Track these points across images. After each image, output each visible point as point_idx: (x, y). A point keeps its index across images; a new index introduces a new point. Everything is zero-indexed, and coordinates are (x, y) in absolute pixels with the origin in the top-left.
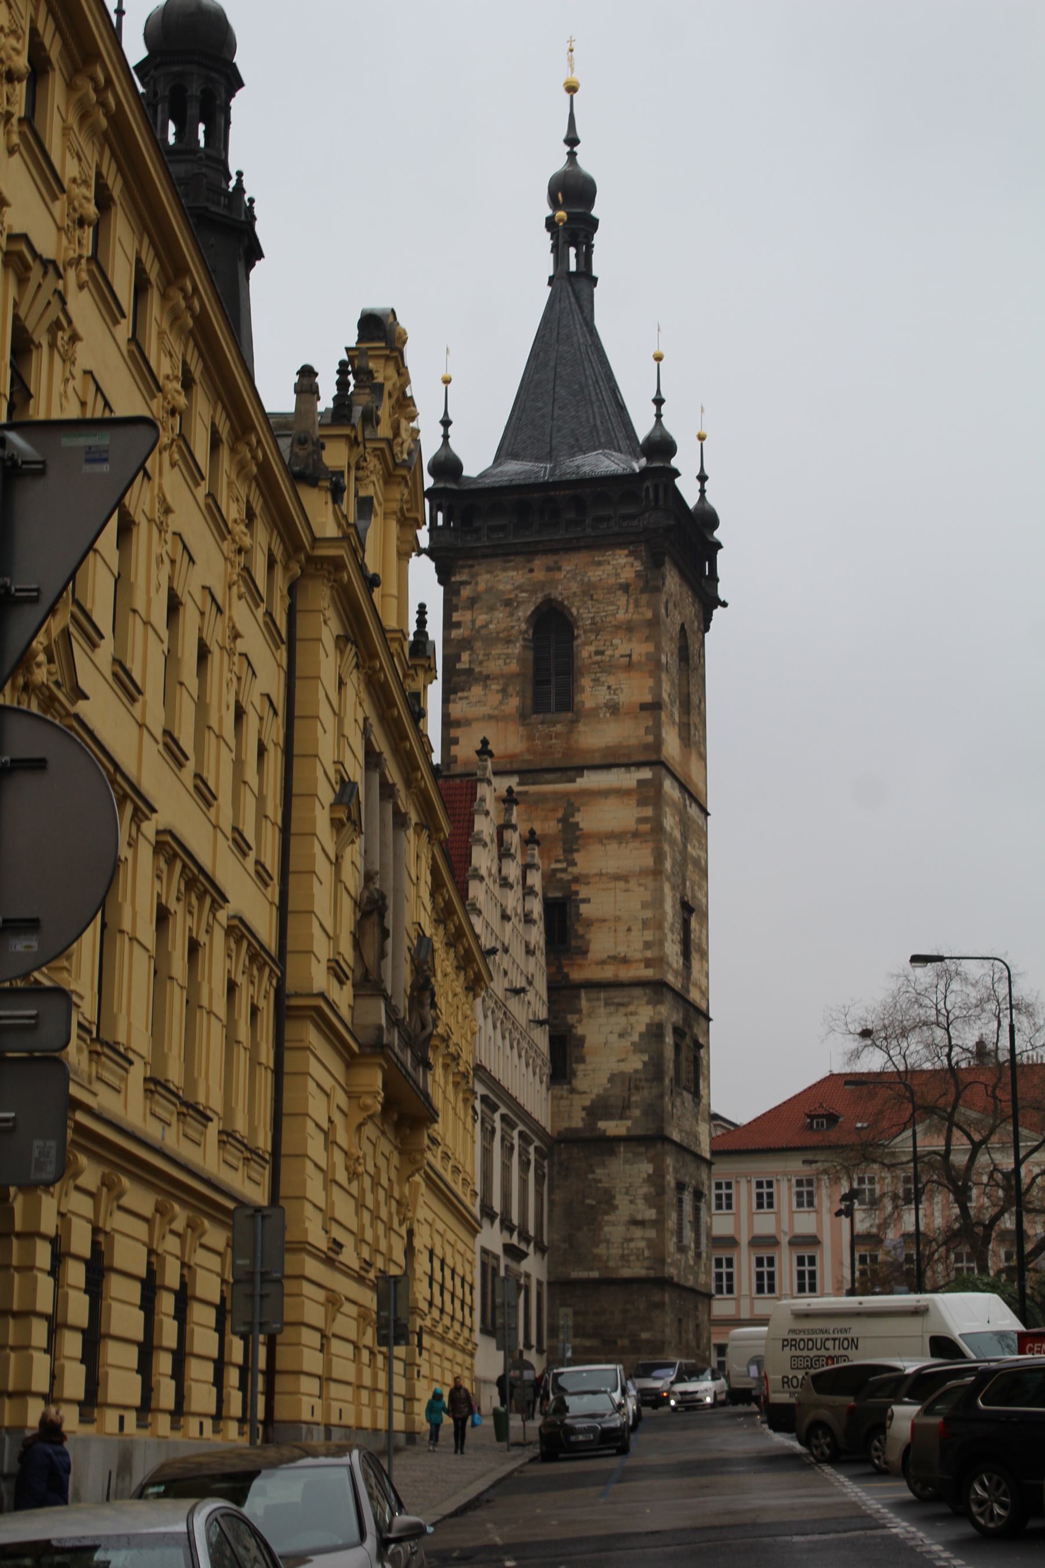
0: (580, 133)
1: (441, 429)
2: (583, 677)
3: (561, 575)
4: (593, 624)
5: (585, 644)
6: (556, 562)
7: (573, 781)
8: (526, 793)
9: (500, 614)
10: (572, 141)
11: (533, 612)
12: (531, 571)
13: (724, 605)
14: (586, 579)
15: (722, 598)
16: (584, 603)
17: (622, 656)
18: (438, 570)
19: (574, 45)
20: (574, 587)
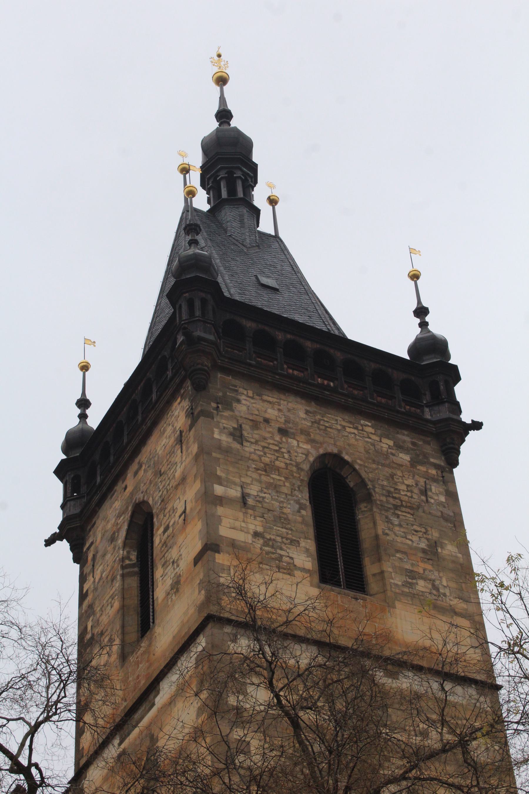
1: (78, 411)
2: (157, 569)
3: (141, 473)
4: (163, 501)
5: (158, 529)
6: (139, 463)
7: (153, 704)
9: (108, 556)
11: (128, 531)
12: (125, 488)
13: (477, 426)
14: (156, 459)
15: (466, 417)
16: (156, 484)
17: (180, 516)
18: (72, 549)
19: (221, 52)
20: (150, 474)
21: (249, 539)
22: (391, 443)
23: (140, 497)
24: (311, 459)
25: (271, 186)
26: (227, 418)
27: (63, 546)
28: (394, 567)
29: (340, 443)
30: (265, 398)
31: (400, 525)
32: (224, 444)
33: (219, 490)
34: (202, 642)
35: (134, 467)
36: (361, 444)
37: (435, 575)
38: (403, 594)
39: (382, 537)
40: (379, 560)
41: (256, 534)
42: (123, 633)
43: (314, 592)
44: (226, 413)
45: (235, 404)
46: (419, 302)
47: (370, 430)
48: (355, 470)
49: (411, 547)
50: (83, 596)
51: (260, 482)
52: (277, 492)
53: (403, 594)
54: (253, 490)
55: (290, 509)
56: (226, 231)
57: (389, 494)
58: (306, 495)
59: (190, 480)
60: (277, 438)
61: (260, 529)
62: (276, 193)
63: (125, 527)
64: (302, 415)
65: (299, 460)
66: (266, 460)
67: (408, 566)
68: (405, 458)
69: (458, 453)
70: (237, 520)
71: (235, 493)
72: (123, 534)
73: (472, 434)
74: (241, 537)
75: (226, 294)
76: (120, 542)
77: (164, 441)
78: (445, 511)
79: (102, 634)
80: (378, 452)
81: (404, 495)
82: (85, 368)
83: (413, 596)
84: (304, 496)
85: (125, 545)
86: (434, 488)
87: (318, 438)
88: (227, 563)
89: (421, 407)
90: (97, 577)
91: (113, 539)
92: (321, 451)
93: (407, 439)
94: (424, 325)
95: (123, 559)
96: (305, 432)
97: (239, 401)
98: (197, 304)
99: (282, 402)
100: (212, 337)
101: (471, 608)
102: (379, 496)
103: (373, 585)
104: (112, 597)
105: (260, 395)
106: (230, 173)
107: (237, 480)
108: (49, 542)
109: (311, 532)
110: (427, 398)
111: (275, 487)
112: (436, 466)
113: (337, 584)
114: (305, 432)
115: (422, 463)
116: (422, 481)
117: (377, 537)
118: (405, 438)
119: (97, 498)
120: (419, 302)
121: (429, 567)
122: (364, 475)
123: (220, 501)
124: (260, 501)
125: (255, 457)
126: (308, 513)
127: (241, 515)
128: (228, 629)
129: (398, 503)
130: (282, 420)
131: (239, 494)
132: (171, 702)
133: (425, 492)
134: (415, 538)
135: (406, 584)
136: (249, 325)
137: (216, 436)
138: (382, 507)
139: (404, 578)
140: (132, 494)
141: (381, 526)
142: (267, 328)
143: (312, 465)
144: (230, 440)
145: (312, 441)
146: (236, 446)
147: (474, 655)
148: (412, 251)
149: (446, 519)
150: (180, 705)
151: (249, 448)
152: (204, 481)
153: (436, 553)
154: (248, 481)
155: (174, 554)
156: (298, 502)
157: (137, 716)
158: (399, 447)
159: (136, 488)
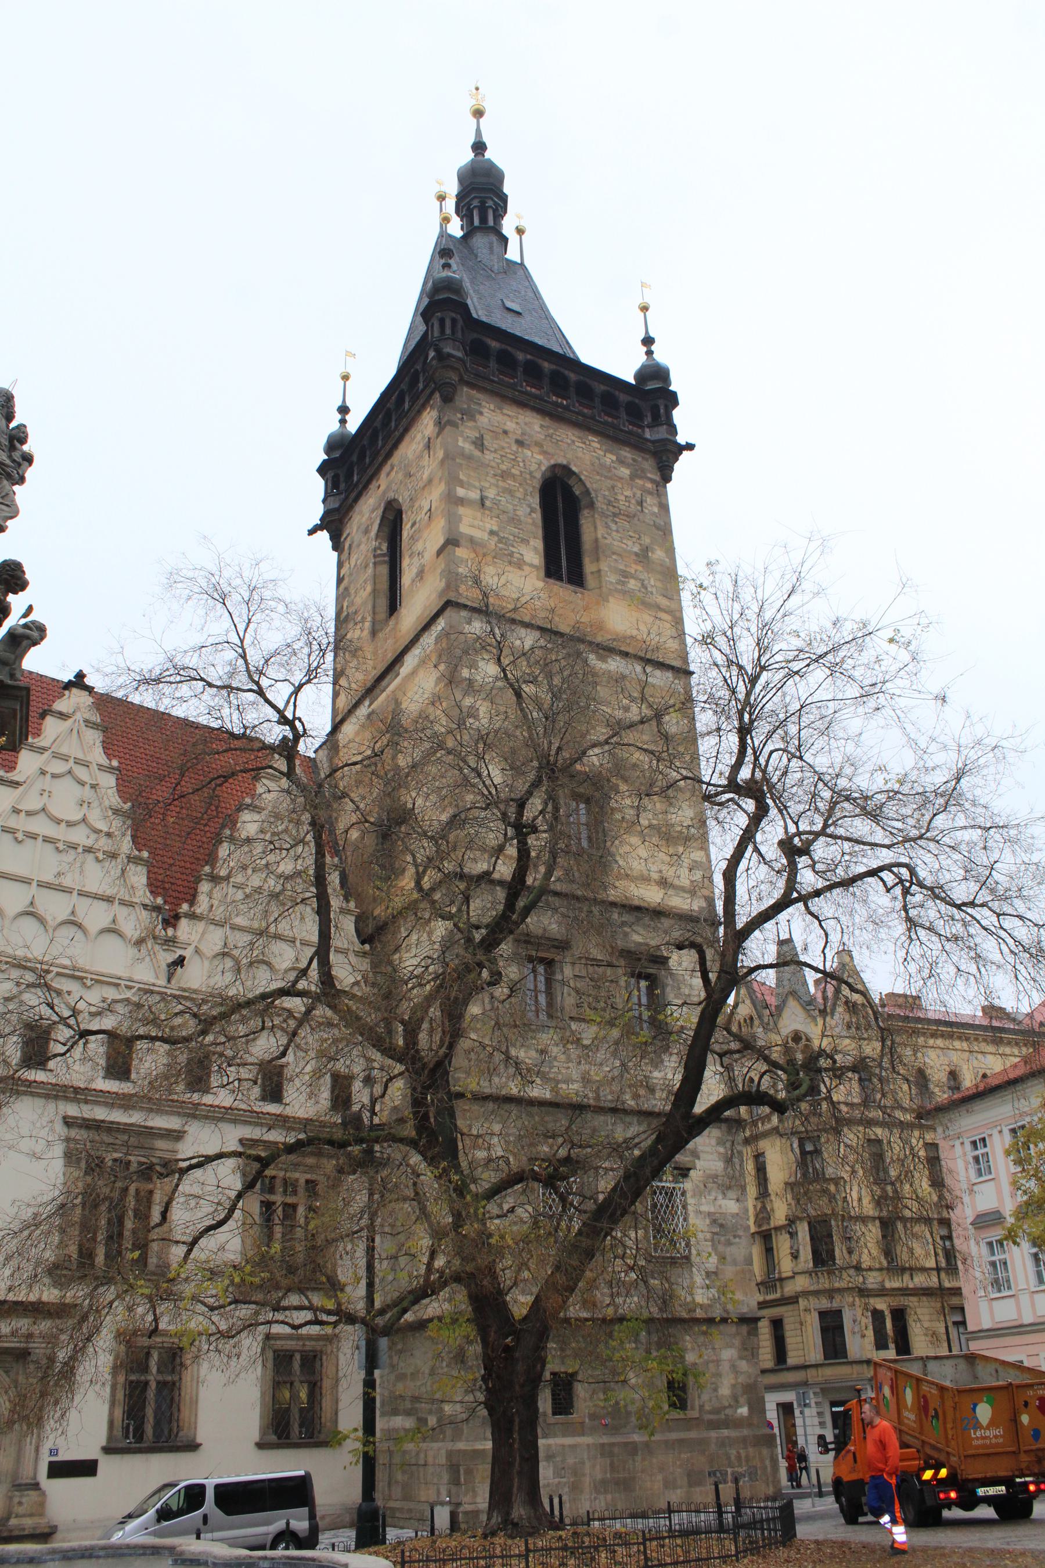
3: (393, 474)
8: (373, 712)
9: (363, 547)
10: (479, 147)
11: (380, 525)
13: (690, 447)
15: (681, 439)
18: (331, 539)
20: (400, 476)
21: (486, 537)
22: (614, 458)
23: (391, 495)
24: (543, 468)
25: (519, 217)
26: (470, 428)
27: (324, 536)
28: (610, 567)
29: (569, 456)
31: (617, 531)
32: (467, 451)
33: (461, 492)
34: (441, 624)
35: (386, 468)
36: (587, 457)
37: (644, 576)
38: (616, 590)
39: (602, 541)
40: (598, 560)
41: (492, 533)
42: (374, 613)
43: (540, 584)
44: (470, 424)
45: (478, 416)
46: (647, 332)
48: (580, 480)
49: (625, 550)
50: (340, 580)
51: (497, 486)
53: (616, 590)
54: (491, 493)
55: (522, 511)
56: (476, 256)
57: (609, 503)
58: (537, 500)
59: (436, 481)
60: (514, 447)
61: (495, 528)
62: (523, 223)
63: (378, 522)
64: (537, 428)
65: (534, 467)
66: (504, 467)
67: (622, 567)
68: (625, 472)
69: (672, 470)
70: (475, 519)
71: (474, 495)
73: (685, 453)
74: (478, 534)
75: (475, 315)
76: (373, 533)
77: (414, 446)
78: (658, 521)
79: (356, 613)
80: (602, 466)
81: (622, 504)
82: (346, 378)
83: (624, 593)
84: (535, 501)
85: (377, 536)
86: (649, 500)
87: (551, 450)
88: (465, 556)
89: (642, 427)
90: (353, 564)
91: (367, 531)
92: (552, 462)
93: (629, 455)
94: (649, 353)
95: (375, 550)
96: (538, 444)
97: (481, 413)
98: (448, 323)
100: (459, 354)
101: (673, 606)
102: (600, 504)
103: (590, 581)
104: (365, 582)
105: (500, 409)
106: (483, 203)
107: (477, 484)
109: (540, 533)
110: (648, 420)
111: (510, 492)
112: (652, 481)
113: (560, 579)
114: (538, 444)
115: (641, 478)
116: (639, 493)
117: (596, 540)
118: (627, 454)
119: (353, 495)
120: (647, 332)
121: (640, 568)
122: (588, 485)
123: (461, 501)
124: (497, 503)
125: (493, 464)
126: (538, 516)
127: (479, 514)
128: (464, 613)
129: (617, 511)
130: (519, 432)
131: (478, 497)
132: (414, 672)
133: (641, 503)
134: (630, 543)
135: (619, 582)
136: (494, 344)
137: (460, 444)
138: (603, 514)
139: (618, 577)
140: (384, 493)
141: (601, 532)
142: (509, 349)
143: (543, 474)
144: (472, 448)
145: (544, 453)
146: (477, 453)
147: (673, 645)
148: (643, 285)
149: (658, 528)
150: (421, 673)
151: (489, 456)
152: (448, 484)
153: (646, 557)
154: (487, 485)
155: (419, 546)
156: (529, 506)
157: (384, 683)
158: (621, 462)
159: (388, 488)
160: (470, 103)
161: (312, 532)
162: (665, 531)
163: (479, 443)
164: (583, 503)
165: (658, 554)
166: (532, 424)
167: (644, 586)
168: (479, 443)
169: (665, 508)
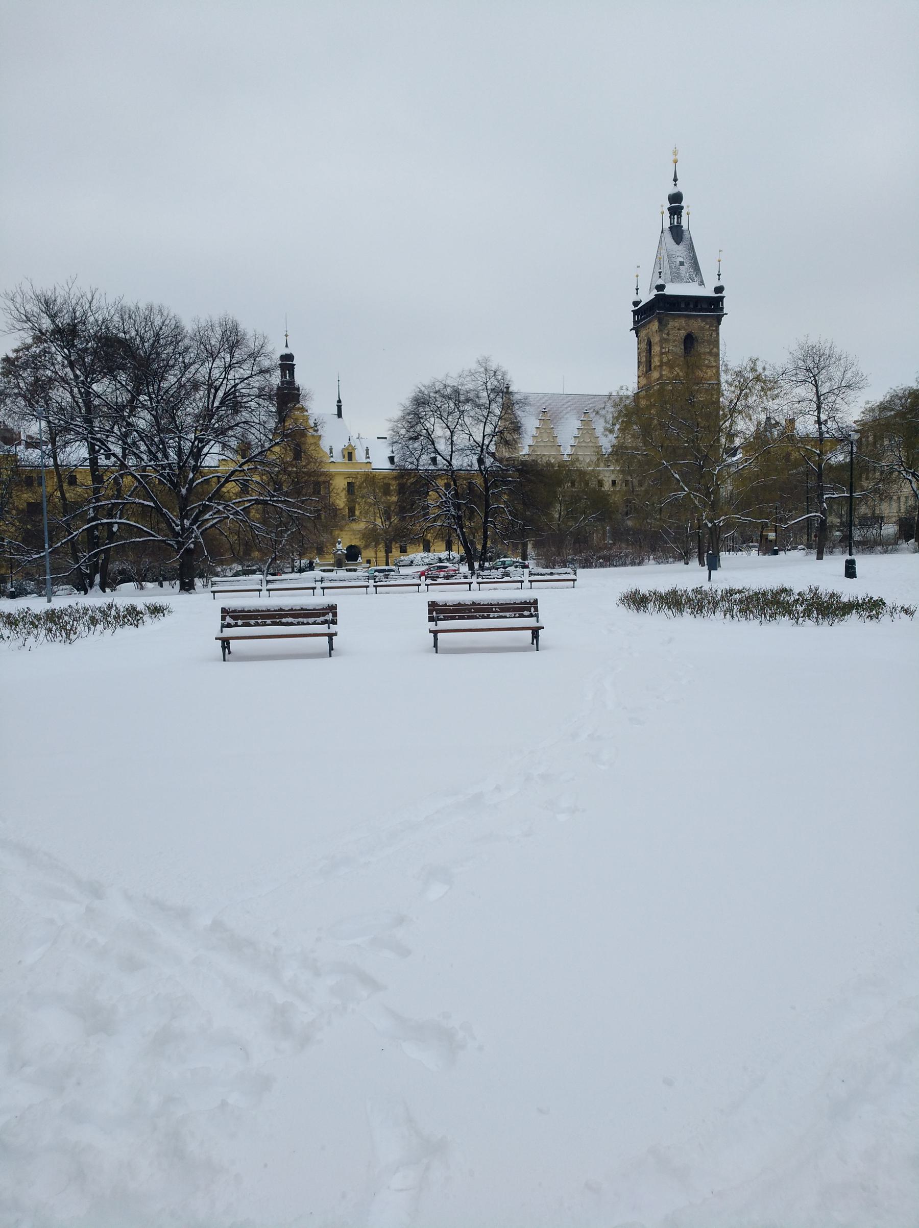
0: (678, 178)
13: (726, 314)
18: (636, 333)
30: (676, 320)
33: (663, 350)
44: (666, 329)
47: (700, 321)
52: (676, 347)
64: (683, 322)
72: (646, 341)
73: (725, 315)
99: (680, 321)
102: (700, 340)
108: (631, 330)
111: (676, 346)
123: (664, 353)
133: (711, 336)
141: (699, 349)
145: (685, 330)
146: (668, 337)
160: (673, 157)
161: (631, 330)
162: (716, 343)
163: (668, 334)
164: (695, 339)
165: (715, 350)
166: (683, 322)
167: (710, 361)
168: (668, 334)
169: (718, 334)
